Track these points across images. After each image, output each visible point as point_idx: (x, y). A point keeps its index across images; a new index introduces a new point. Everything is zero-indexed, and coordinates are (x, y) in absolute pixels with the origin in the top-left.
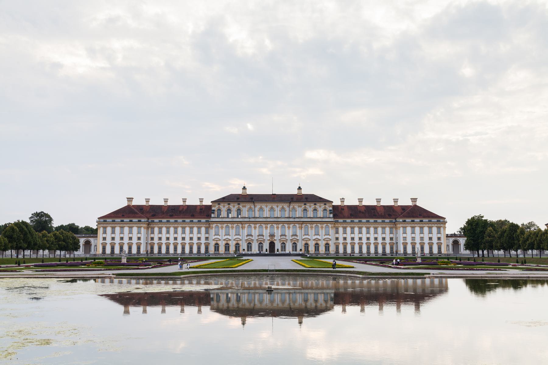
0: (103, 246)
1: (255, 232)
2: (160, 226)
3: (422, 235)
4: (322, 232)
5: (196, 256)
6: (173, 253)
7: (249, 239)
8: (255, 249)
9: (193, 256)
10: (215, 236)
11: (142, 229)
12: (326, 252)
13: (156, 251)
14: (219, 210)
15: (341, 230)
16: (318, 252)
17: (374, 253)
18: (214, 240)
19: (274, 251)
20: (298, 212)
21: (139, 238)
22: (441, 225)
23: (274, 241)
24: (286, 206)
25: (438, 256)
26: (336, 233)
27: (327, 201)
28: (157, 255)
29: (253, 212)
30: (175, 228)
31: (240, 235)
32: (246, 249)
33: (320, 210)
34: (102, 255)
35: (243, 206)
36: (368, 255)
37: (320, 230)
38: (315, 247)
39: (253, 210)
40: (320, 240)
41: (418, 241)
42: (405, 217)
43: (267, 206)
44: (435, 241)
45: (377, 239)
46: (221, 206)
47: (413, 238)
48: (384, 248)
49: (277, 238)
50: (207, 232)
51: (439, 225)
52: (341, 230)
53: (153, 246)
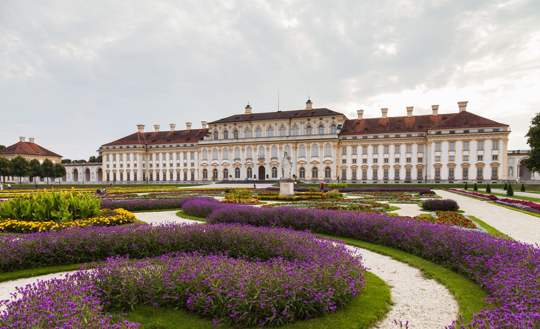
1: (243, 156)
2: (157, 151)
3: (466, 153)
4: (321, 153)
5: (190, 183)
6: (169, 180)
7: (237, 164)
8: (243, 176)
9: (187, 183)
10: (203, 161)
11: (138, 155)
12: (327, 178)
13: (155, 178)
14: (216, 132)
15: (349, 149)
16: (316, 179)
17: (393, 179)
18: (202, 165)
20: (300, 129)
21: (135, 165)
22: (500, 137)
23: (264, 166)
24: (285, 123)
25: (491, 183)
28: (156, 182)
29: (251, 133)
30: (170, 154)
31: (228, 160)
32: (233, 175)
33: (327, 126)
35: (240, 127)
37: (319, 150)
38: (313, 172)
40: (318, 163)
41: (459, 161)
42: (440, 127)
43: (264, 125)
44: (488, 160)
45: (356, 162)
46: (218, 128)
47: (438, 158)
48: (408, 173)
49: (267, 161)
51: (497, 137)
52: (349, 149)
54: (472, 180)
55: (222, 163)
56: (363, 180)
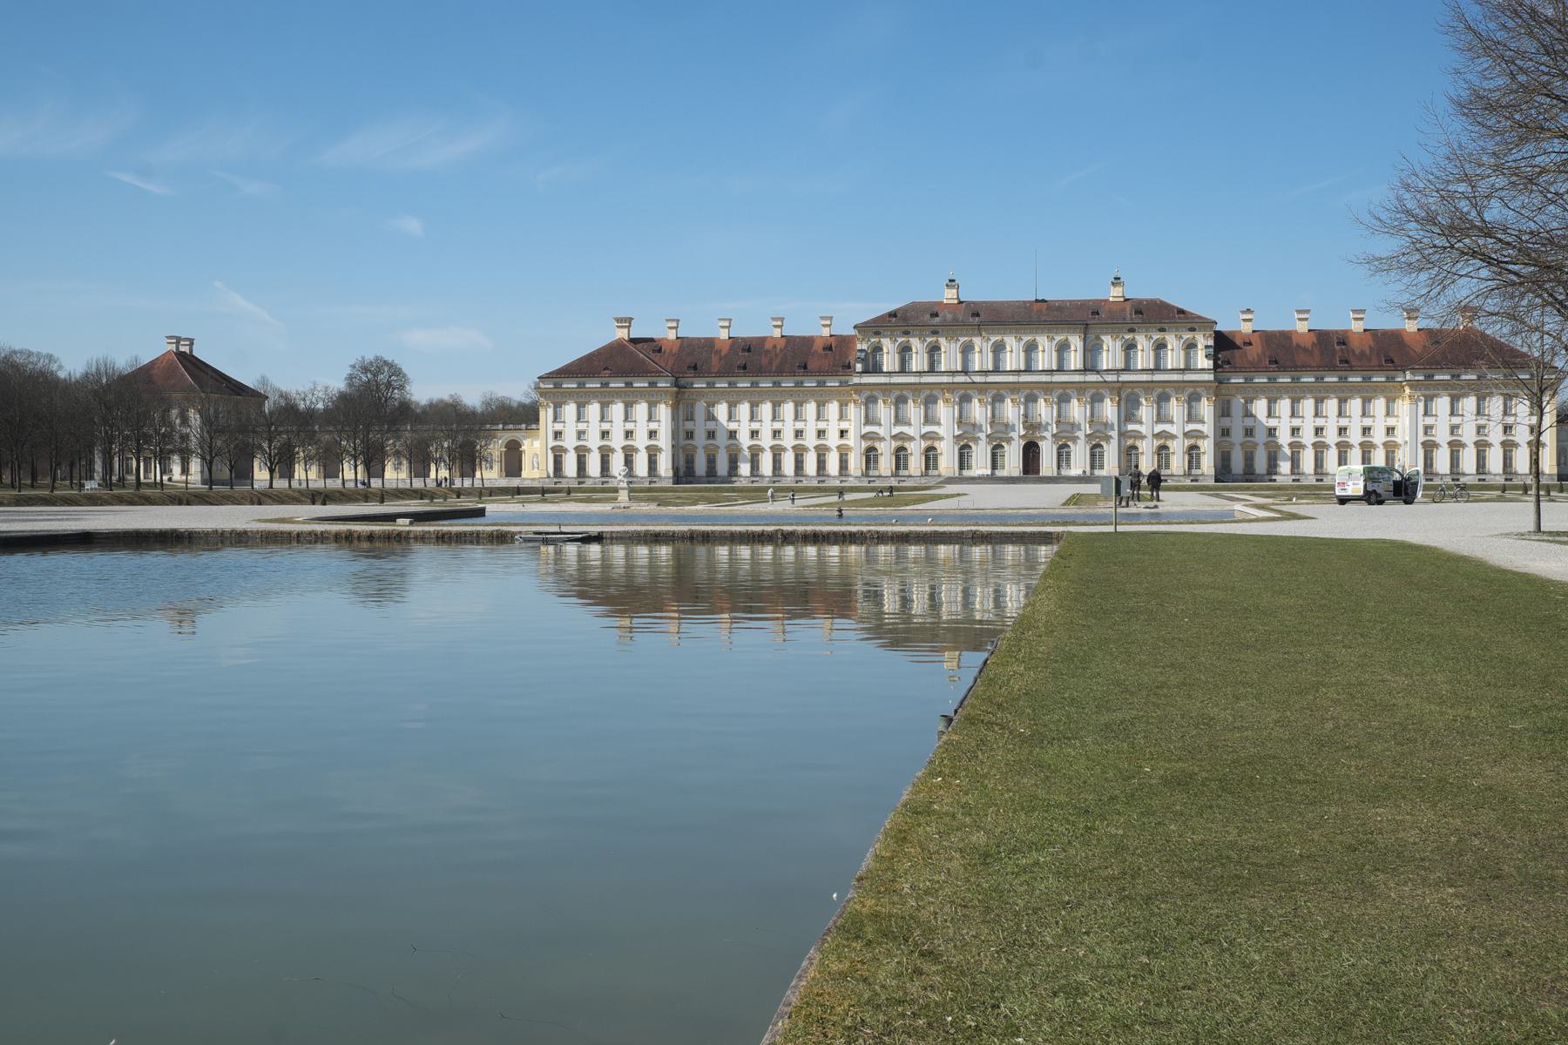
0: (555, 457)
5: (815, 483)
9: (805, 483)
18: (864, 437)
19: (1038, 472)
21: (652, 434)
23: (1040, 444)
26: (1223, 416)
27: (1196, 320)
28: (705, 479)
34: (556, 480)
36: (1317, 480)
39: (977, 349)
41: (1468, 435)
50: (842, 417)
53: (692, 456)
54: (1495, 475)
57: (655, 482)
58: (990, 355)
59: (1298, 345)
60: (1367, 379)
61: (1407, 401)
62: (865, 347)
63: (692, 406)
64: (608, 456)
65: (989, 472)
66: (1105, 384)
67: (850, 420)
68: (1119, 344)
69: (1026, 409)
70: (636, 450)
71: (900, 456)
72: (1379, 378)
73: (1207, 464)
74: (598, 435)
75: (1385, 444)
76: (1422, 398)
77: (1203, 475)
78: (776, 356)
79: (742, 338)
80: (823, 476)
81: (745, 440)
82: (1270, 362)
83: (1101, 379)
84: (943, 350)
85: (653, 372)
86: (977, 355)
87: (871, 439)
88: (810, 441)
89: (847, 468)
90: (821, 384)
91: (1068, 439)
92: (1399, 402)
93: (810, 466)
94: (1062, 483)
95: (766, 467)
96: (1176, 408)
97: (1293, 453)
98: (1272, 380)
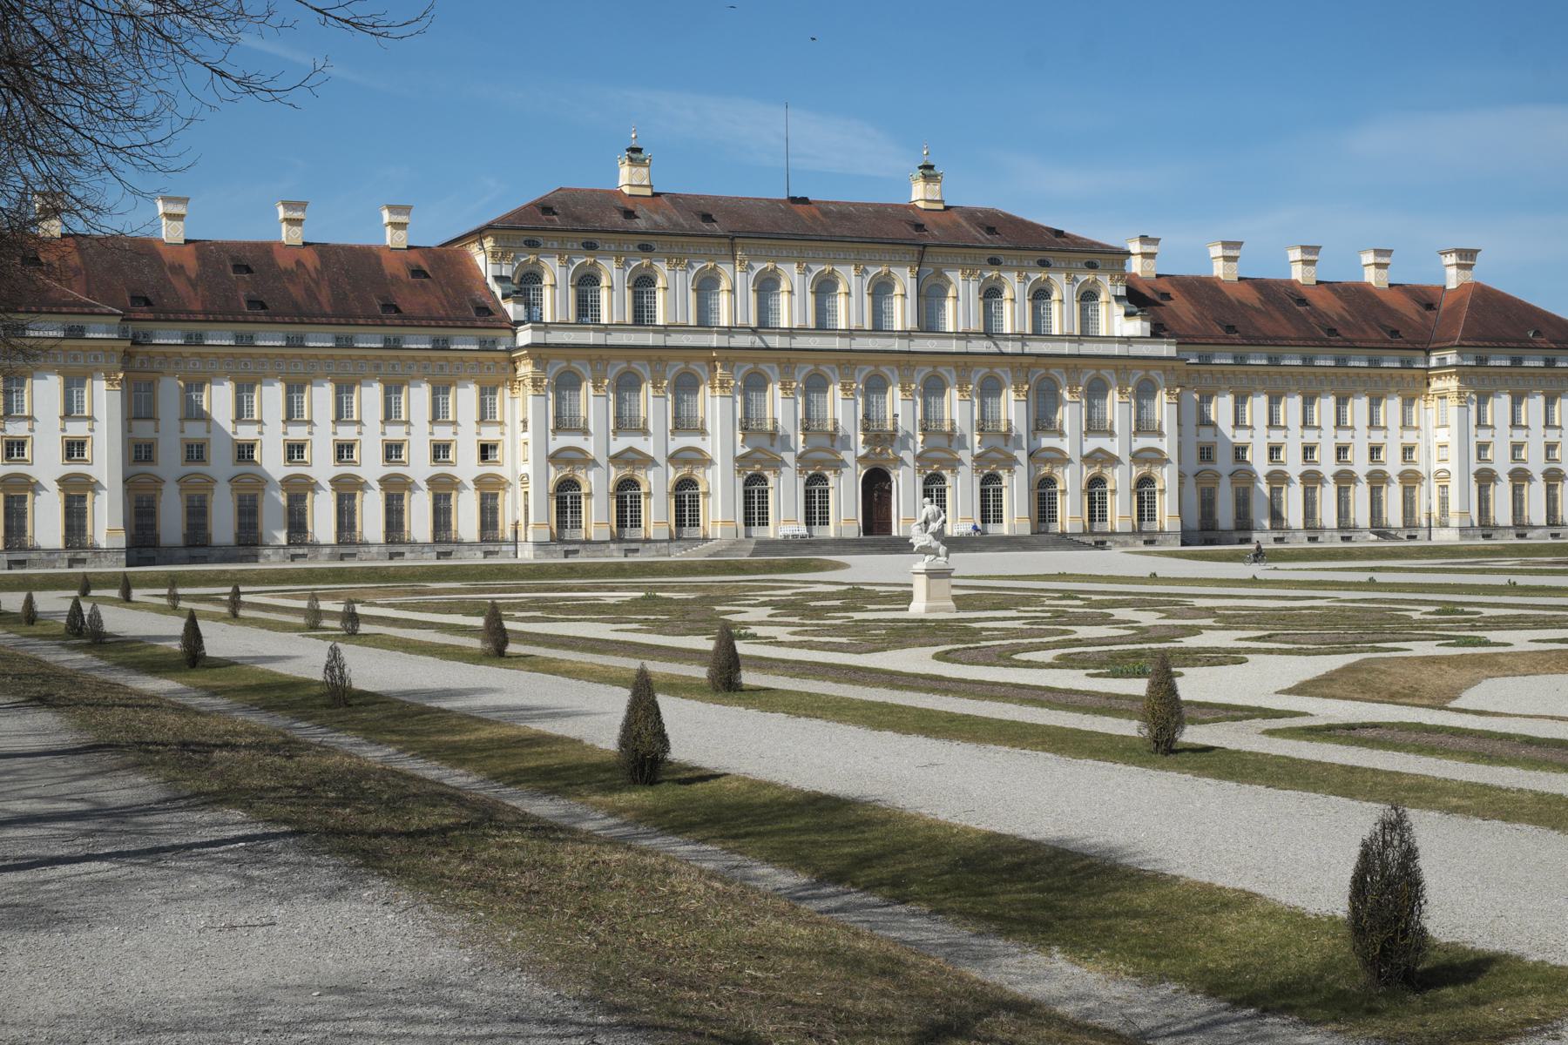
5: (430, 560)
9: (409, 561)
19: (887, 527)
21: (74, 449)
27: (1097, 248)
28: (184, 553)
39: (725, 285)
55: (670, 452)
56: (1238, 529)
57: (83, 561)
58: (753, 297)
59: (1239, 301)
60: (1374, 363)
61: (1452, 405)
62: (506, 271)
63: (151, 386)
64: (23, 499)
65: (802, 530)
66: (999, 359)
67: (501, 423)
68: (974, 287)
69: (867, 405)
70: (34, 486)
71: (626, 497)
72: (1391, 362)
73: (1166, 512)
74: (58, 450)
75: (1403, 476)
76: (1474, 397)
77: (1162, 531)
78: (317, 284)
79: (216, 244)
80: (449, 542)
81: (272, 462)
82: (1230, 329)
83: (993, 349)
84: (660, 283)
85: (66, 304)
86: (724, 300)
87: (570, 462)
88: (419, 466)
89: (494, 525)
90: (441, 345)
91: (826, 464)
92: (1419, 404)
93: (419, 522)
94: (982, 550)
95: (322, 520)
96: (1116, 407)
97: (1272, 490)
98: (1240, 361)
